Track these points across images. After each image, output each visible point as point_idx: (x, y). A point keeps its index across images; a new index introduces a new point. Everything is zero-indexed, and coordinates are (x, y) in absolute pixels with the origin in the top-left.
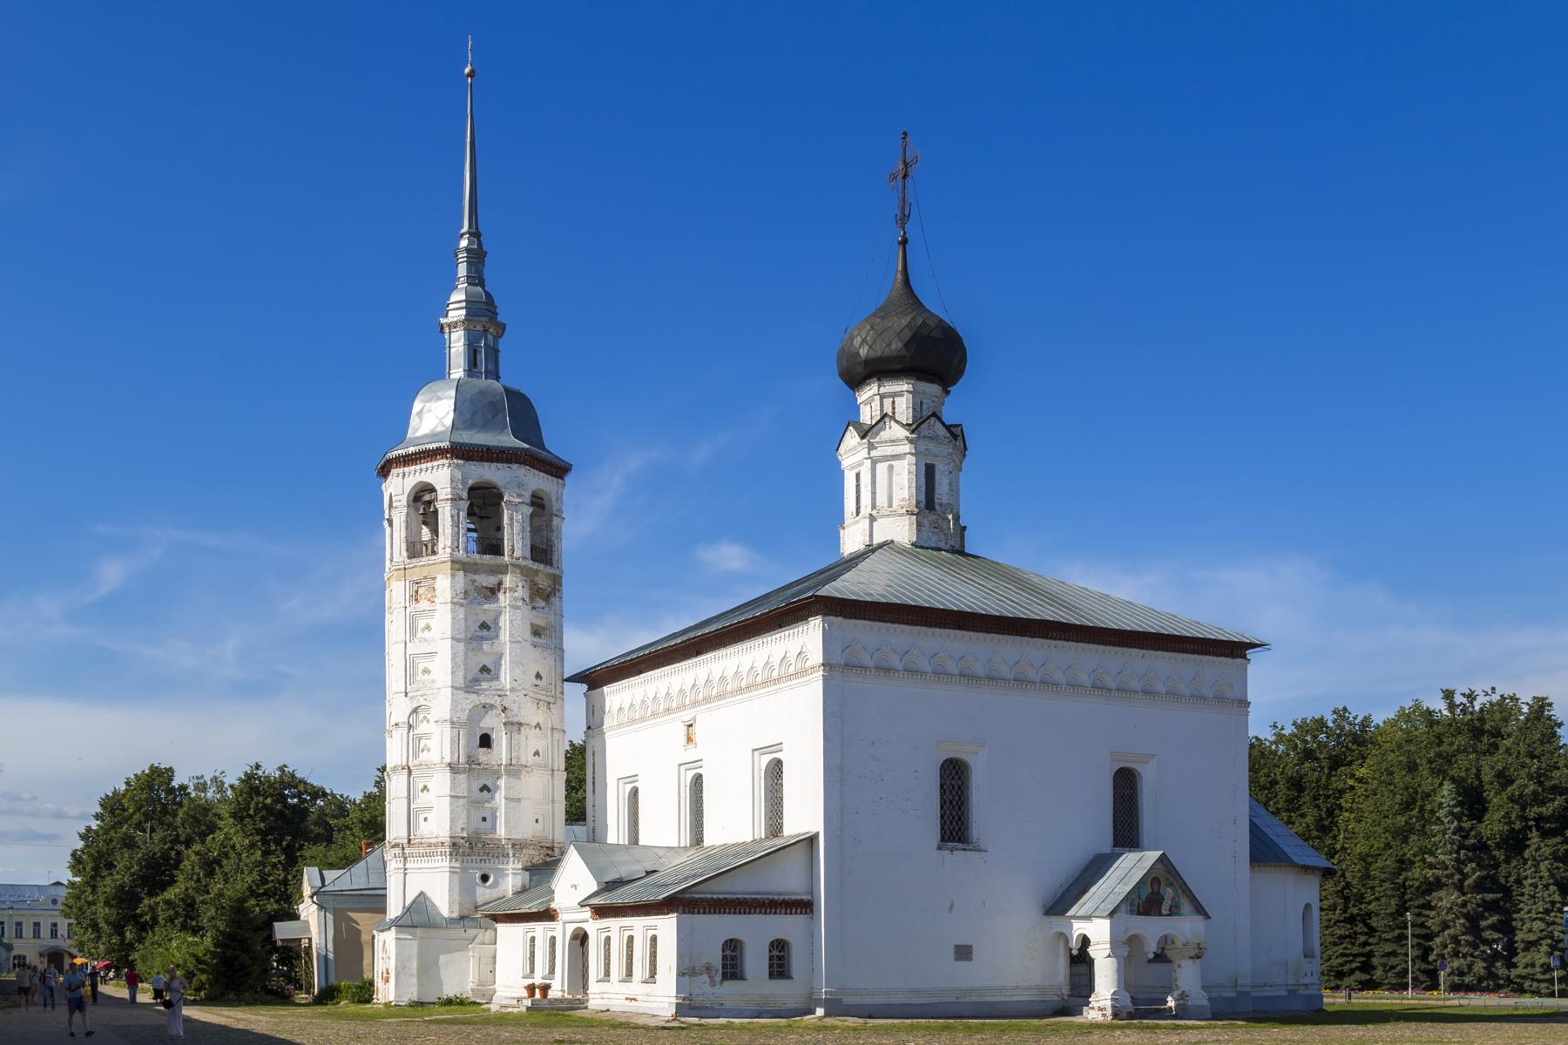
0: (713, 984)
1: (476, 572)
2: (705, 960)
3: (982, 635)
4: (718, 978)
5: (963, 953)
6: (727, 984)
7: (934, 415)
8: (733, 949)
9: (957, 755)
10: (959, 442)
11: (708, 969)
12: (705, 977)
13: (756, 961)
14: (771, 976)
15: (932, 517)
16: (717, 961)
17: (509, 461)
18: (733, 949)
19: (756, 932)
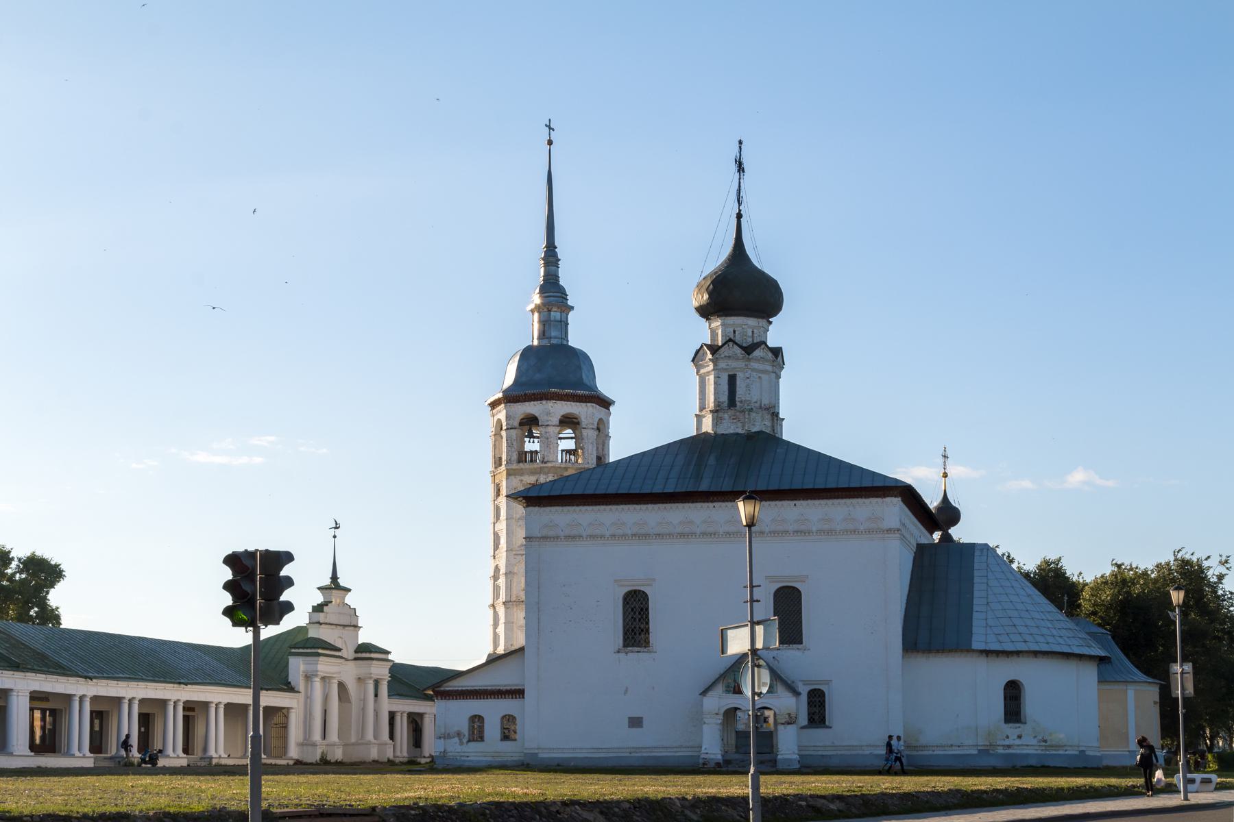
0: (461, 743)
1: (522, 474)
2: (456, 729)
3: (650, 506)
4: (465, 741)
5: (636, 722)
6: (472, 744)
7: (730, 340)
8: (477, 722)
9: (642, 589)
10: (758, 353)
11: (459, 734)
12: (456, 739)
13: (492, 729)
14: (505, 737)
15: (731, 412)
16: (465, 730)
17: (541, 399)
18: (477, 722)
19: (493, 711)
